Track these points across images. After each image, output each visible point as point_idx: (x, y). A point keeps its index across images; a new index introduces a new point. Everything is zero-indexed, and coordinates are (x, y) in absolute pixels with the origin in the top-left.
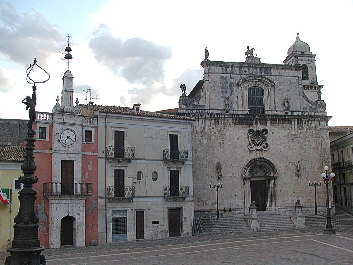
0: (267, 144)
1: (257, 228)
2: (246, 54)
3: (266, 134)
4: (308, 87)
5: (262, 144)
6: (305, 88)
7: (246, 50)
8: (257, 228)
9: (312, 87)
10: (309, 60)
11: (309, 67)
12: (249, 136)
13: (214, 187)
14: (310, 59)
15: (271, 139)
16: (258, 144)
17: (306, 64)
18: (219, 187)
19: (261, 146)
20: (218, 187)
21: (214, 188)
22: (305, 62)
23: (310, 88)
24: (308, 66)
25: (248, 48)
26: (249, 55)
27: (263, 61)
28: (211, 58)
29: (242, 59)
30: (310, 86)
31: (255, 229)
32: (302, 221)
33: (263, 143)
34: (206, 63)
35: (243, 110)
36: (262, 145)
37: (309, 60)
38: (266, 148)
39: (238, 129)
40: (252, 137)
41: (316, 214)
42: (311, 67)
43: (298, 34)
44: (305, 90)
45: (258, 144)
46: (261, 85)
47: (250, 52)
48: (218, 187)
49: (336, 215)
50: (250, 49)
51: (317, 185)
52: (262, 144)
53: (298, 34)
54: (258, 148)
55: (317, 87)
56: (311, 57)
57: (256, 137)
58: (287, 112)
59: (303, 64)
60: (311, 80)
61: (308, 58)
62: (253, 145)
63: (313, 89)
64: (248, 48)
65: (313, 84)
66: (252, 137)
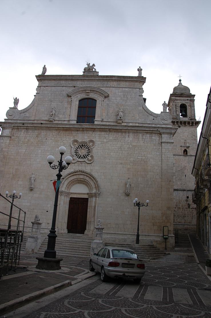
0: (92, 157)
1: (33, 249)
3: (93, 146)
4: (185, 123)
5: (87, 156)
6: (182, 124)
8: (33, 249)
9: (189, 123)
10: (187, 100)
11: (187, 106)
12: (72, 147)
14: (189, 99)
15: (96, 151)
16: (82, 156)
17: (185, 103)
18: (17, 197)
19: (85, 158)
21: (10, 197)
22: (184, 101)
23: (187, 124)
24: (187, 105)
25: (88, 65)
30: (187, 122)
31: (31, 250)
33: (88, 156)
34: (42, 78)
35: (69, 121)
36: (87, 157)
37: (187, 100)
39: (61, 140)
40: (76, 149)
41: (138, 241)
42: (190, 106)
43: (180, 81)
44: (182, 125)
45: (82, 156)
46: (92, 95)
50: (91, 65)
52: (87, 156)
53: (180, 81)
54: (80, 160)
55: (194, 122)
56: (190, 97)
57: (80, 148)
59: (182, 103)
60: (190, 118)
61: (187, 98)
62: (75, 157)
63: (191, 124)
64: (88, 65)
65: (191, 120)
66: (76, 149)
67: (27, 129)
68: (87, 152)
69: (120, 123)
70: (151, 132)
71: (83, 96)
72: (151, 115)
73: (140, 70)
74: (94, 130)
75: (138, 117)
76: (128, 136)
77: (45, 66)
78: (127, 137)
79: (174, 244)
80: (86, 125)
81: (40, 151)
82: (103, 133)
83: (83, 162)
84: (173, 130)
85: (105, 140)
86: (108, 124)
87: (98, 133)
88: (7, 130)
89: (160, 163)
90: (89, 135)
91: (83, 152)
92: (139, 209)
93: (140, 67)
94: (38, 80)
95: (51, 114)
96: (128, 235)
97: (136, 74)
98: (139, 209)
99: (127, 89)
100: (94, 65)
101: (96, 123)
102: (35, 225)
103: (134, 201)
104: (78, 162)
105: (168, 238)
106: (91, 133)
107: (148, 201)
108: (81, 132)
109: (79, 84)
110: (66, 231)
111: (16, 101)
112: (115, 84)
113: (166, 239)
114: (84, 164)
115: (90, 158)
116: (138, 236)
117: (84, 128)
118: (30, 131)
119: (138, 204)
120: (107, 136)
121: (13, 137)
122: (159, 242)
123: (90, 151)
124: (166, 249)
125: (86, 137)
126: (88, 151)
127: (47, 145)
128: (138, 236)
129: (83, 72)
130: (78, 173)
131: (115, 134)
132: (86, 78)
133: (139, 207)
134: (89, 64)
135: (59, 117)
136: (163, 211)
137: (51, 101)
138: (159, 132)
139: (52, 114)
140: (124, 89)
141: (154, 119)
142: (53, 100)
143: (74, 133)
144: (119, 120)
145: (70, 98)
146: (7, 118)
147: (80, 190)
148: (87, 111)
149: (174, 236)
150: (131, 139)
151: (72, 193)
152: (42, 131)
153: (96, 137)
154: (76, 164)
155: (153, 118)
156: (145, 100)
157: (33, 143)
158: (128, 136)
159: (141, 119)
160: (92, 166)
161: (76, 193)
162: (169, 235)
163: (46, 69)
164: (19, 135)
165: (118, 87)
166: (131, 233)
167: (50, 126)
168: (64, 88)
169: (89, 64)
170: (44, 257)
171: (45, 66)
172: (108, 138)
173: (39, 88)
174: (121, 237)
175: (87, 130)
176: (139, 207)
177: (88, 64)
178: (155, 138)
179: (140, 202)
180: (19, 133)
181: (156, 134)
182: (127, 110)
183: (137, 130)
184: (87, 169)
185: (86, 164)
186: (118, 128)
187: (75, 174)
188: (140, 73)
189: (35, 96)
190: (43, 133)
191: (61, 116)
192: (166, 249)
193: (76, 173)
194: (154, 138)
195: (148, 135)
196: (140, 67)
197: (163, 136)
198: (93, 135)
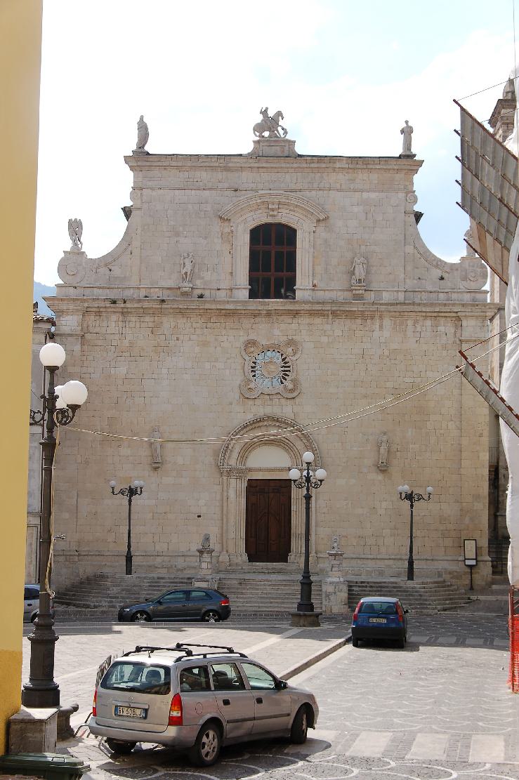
0: (295, 381)
2: (259, 128)
3: (295, 354)
7: (259, 118)
13: (122, 492)
15: (304, 366)
20: (132, 492)
25: (264, 113)
26: (266, 134)
27: (300, 149)
28: (151, 148)
29: (243, 143)
32: (338, 593)
34: (141, 159)
38: (292, 391)
39: (216, 340)
47: (270, 123)
48: (132, 492)
49: (494, 587)
50: (271, 113)
51: (419, 500)
58: (357, 292)
64: (264, 113)
67: (122, 313)
68: (283, 369)
69: (359, 297)
70: (435, 314)
71: (262, 218)
72: (437, 266)
73: (407, 132)
74: (295, 314)
75: (403, 276)
76: (381, 327)
77: (142, 118)
78: (378, 326)
79: (490, 577)
80: (274, 304)
81: (165, 371)
82: (318, 320)
83: (275, 397)
84: (490, 310)
85: (324, 339)
86: (328, 296)
87: (304, 320)
88: (69, 318)
89: (456, 392)
90: (283, 326)
91: (273, 370)
92: (412, 506)
93: (407, 122)
94: (132, 168)
95: (183, 272)
96: (386, 561)
97: (397, 151)
98: (412, 506)
99: (373, 195)
100: (279, 114)
101: (298, 294)
102: (205, 555)
103: (400, 488)
104: (262, 396)
105: (477, 565)
106: (288, 319)
107: (430, 489)
108: (263, 319)
109: (246, 179)
110: (245, 557)
111: (75, 228)
112: (340, 178)
113: (471, 567)
114: (277, 400)
115: (290, 386)
116: (411, 563)
117: (271, 310)
118: (133, 319)
119: (410, 497)
120: (329, 327)
121: (88, 336)
122: (455, 574)
123: (289, 367)
124: (472, 588)
125: (277, 332)
126: (285, 367)
127: (181, 354)
128: (411, 563)
129: (254, 142)
130: (265, 423)
131: (348, 322)
132: (264, 165)
133: (412, 502)
134: (266, 110)
135: (203, 278)
136: (464, 504)
137: (177, 234)
138: (454, 315)
139: (186, 273)
140: (365, 195)
141: (442, 278)
142: (181, 229)
143: (247, 323)
144: (359, 286)
145: (226, 224)
146: (61, 282)
147: (269, 462)
148: (273, 261)
149: (490, 559)
150: (386, 333)
151: (250, 470)
152: (165, 319)
153: (301, 330)
154: (258, 402)
155: (439, 273)
156: (418, 216)
157: (143, 350)
158: (381, 327)
159: (410, 278)
160: (297, 403)
161: (260, 470)
162: (479, 559)
163: (146, 129)
164: (103, 330)
165: (349, 190)
166: (393, 557)
167: (187, 302)
168: (207, 193)
169: (266, 110)
170: (299, 609)
171: (142, 118)
172: (331, 333)
173: (139, 192)
174: (371, 565)
175: (279, 313)
176: (412, 502)
177: (263, 110)
178: (446, 327)
179: (412, 492)
180: (105, 324)
181: (449, 319)
182: (375, 254)
183: (403, 310)
184: (285, 410)
185: (283, 401)
186: (356, 306)
187: (257, 425)
188: (408, 144)
189: (127, 212)
190: (168, 323)
191: (207, 276)
192: (473, 589)
193: (261, 424)
194: (441, 328)
195: (428, 323)
196: (407, 122)
197: (464, 323)
198: (294, 326)
